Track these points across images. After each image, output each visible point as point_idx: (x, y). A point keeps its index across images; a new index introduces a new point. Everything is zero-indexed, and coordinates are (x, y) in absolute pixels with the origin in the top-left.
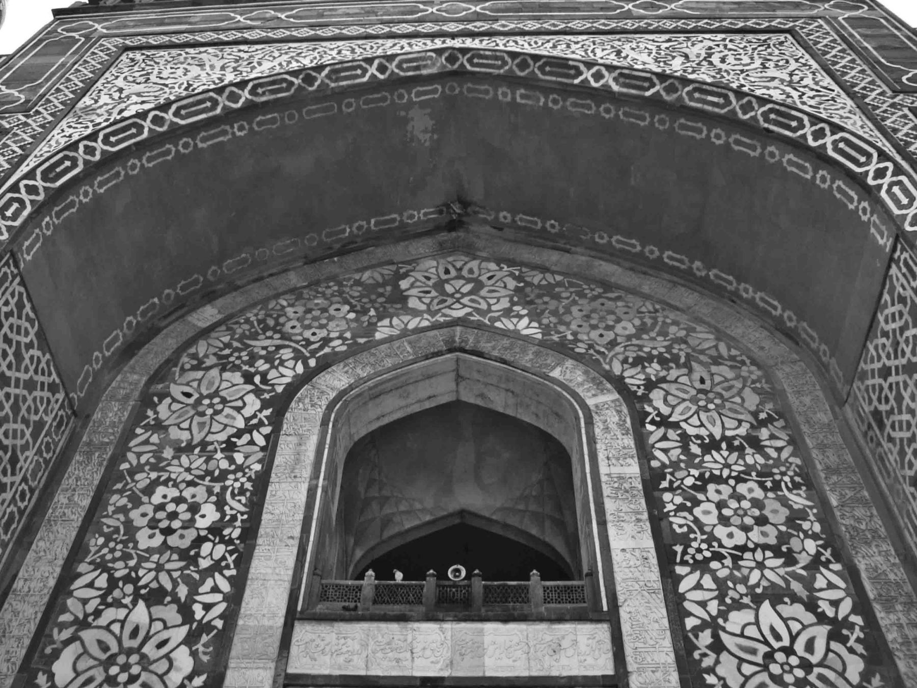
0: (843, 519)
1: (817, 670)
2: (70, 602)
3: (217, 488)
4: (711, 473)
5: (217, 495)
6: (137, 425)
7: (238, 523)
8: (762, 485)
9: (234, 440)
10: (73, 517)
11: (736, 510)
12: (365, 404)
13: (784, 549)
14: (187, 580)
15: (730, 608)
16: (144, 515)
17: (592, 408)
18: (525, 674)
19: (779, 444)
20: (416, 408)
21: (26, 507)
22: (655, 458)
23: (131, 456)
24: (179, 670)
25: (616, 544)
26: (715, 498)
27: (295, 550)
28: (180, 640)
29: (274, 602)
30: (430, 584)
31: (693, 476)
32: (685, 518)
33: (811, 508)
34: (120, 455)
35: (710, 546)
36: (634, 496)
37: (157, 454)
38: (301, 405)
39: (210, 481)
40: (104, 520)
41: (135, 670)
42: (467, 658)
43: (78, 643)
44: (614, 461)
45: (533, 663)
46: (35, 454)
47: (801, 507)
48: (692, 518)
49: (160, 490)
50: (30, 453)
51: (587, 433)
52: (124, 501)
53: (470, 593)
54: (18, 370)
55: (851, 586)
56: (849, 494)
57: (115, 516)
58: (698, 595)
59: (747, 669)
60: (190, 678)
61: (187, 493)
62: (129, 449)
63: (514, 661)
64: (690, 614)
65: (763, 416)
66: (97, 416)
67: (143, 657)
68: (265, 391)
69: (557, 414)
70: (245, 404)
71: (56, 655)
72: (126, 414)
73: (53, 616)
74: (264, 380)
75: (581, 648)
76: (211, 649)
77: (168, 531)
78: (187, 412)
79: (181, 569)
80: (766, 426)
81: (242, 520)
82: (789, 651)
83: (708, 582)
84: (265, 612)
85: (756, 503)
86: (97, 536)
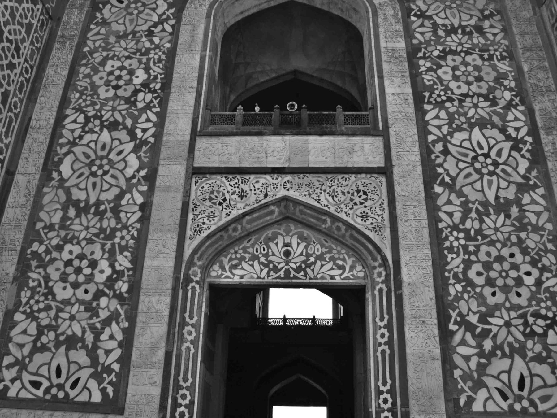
1: (501, 167)
2: (64, 131)
3: (144, 59)
4: (450, 48)
5: (145, 64)
6: (91, 22)
7: (159, 80)
8: (481, 57)
9: (152, 29)
11: (463, 72)
12: (233, 3)
13: (491, 96)
14: (131, 115)
16: (101, 78)
17: (377, 5)
18: (332, 165)
21: (30, 78)
22: (416, 38)
23: (89, 43)
24: (131, 167)
25: (389, 90)
26: (452, 64)
27: (194, 95)
28: (130, 150)
29: (183, 125)
30: (276, 113)
32: (432, 76)
34: (82, 42)
35: (446, 93)
36: (401, 61)
37: (106, 40)
38: (193, 6)
39: (140, 55)
40: (77, 83)
41: (106, 168)
43: (72, 154)
44: (389, 39)
45: (337, 159)
48: (436, 76)
49: (110, 63)
50: (27, 44)
51: (373, 21)
53: (300, 119)
55: (529, 119)
56: (536, 63)
58: (436, 122)
59: (462, 165)
60: (138, 171)
61: (127, 63)
62: (88, 39)
64: (431, 133)
65: (487, 12)
66: (65, 18)
67: (110, 160)
69: (355, 9)
70: (157, 6)
71: (61, 161)
72: (83, 16)
73: (56, 140)
75: (365, 150)
77: (117, 87)
78: (122, 13)
79: (126, 109)
80: (488, 19)
81: (161, 79)
82: (487, 156)
83: (443, 114)
84: (179, 131)
85: (477, 68)
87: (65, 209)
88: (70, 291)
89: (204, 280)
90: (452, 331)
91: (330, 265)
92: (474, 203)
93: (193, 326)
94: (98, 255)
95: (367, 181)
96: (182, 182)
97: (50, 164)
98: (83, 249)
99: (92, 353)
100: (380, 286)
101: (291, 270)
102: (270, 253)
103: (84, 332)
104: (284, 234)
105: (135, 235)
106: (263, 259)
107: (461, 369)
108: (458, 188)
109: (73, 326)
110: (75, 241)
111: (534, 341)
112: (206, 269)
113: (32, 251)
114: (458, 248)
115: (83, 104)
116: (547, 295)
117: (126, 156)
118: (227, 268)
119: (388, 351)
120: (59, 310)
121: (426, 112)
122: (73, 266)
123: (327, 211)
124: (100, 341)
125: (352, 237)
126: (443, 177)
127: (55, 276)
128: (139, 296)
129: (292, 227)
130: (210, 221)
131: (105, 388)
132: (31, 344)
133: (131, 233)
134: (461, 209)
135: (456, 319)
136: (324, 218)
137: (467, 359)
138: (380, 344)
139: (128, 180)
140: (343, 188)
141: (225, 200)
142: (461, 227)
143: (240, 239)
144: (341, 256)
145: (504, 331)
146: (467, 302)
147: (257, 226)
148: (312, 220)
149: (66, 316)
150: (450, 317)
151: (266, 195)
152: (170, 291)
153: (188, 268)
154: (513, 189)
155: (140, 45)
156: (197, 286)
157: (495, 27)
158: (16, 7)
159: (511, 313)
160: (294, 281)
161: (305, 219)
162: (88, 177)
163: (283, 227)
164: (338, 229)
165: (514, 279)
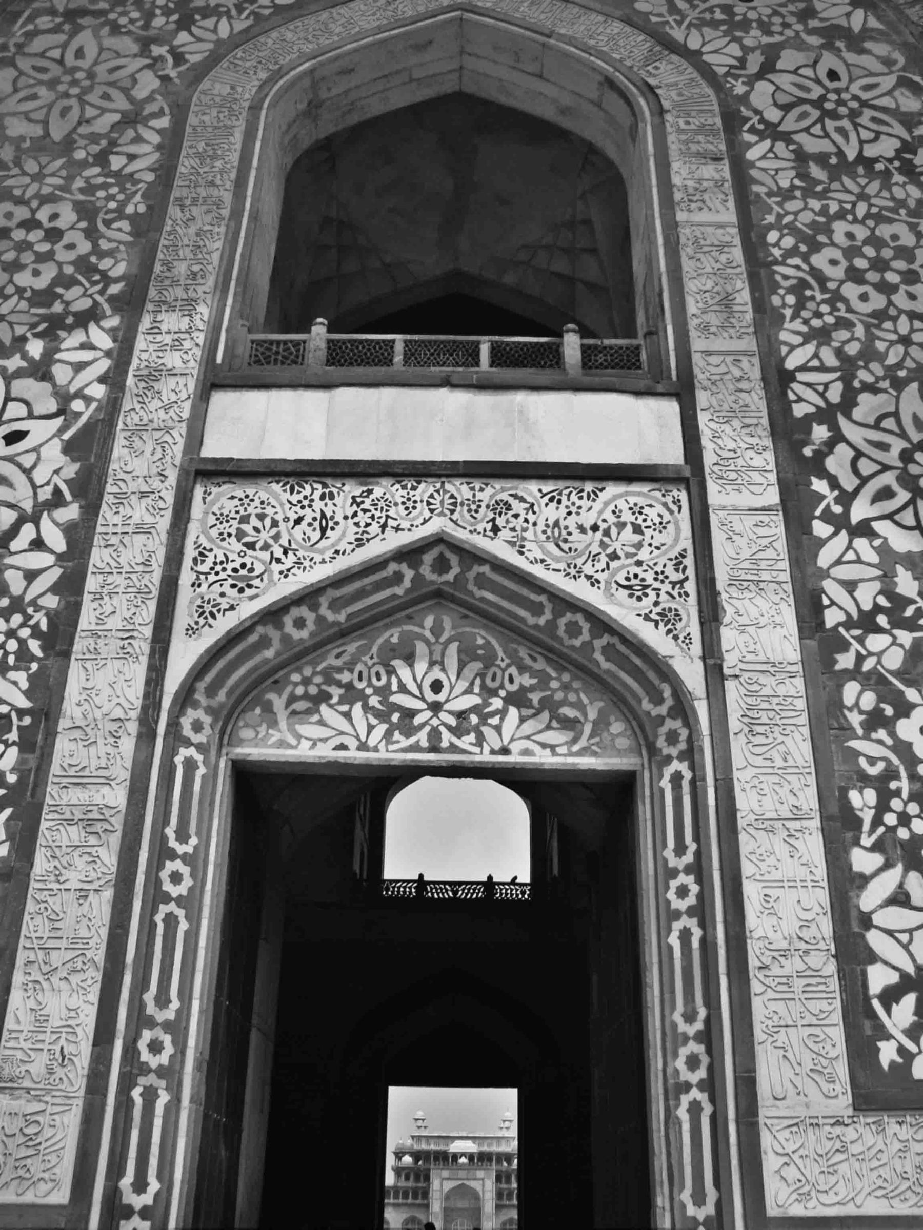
102: (395, 687)
105: (44, 626)
133: (32, 622)
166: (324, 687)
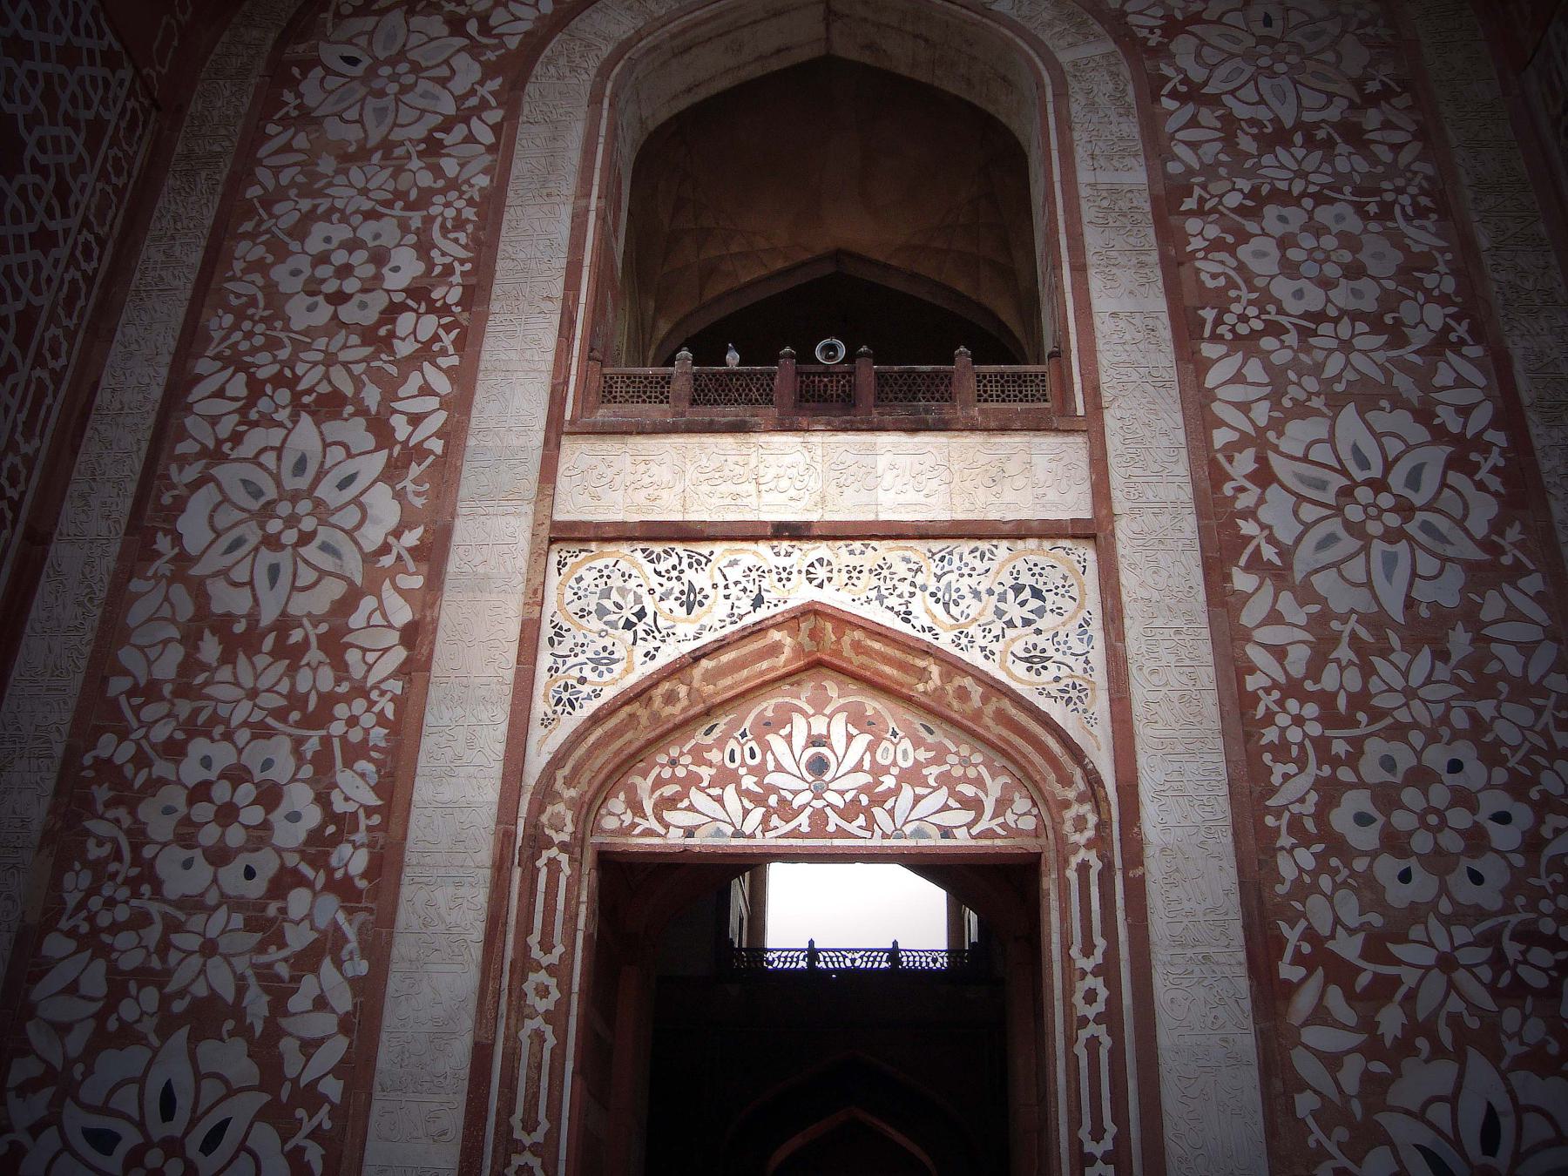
0: (1496, 271)
1: (1420, 516)
2: (189, 422)
3: (416, 220)
5: (417, 232)
7: (456, 279)
8: (1360, 209)
9: (438, 135)
10: (176, 283)
11: (1311, 251)
13: (1388, 319)
14: (378, 377)
15: (1290, 415)
17: (1066, 68)
18: (945, 516)
19: (1397, 137)
20: (756, 71)
21: (96, 271)
22: (1175, 158)
23: (262, 174)
25: (1102, 303)
26: (1277, 229)
27: (556, 319)
30: (784, 371)
31: (1241, 191)
32: (1222, 262)
33: (1442, 251)
34: (242, 176)
35: (1263, 311)
36: (1135, 223)
38: (552, 70)
39: (405, 209)
41: (308, 524)
42: (848, 492)
43: (212, 485)
46: (98, 180)
47: (1426, 249)
48: (1235, 264)
49: (319, 230)
50: (89, 178)
52: (260, 251)
53: (853, 386)
54: (43, 29)
57: (248, 277)
58: (1236, 393)
60: (397, 533)
62: (260, 162)
63: (927, 496)
64: (1221, 423)
65: (1373, 87)
67: (318, 503)
68: (486, 46)
69: (1004, 79)
70: (453, 72)
71: (180, 505)
72: (247, 101)
74: (485, 29)
76: (427, 486)
77: (339, 298)
80: (1376, 105)
82: (1379, 485)
83: (1254, 371)
85: (1349, 241)
86: (220, 312)
87: (191, 639)
88: (202, 872)
89: (583, 839)
90: (1287, 982)
91: (941, 796)
92: (1344, 619)
93: (551, 970)
94: (283, 769)
95: (1043, 561)
96: (522, 563)
97: (151, 512)
98: (240, 751)
99: (265, 1049)
100: (1082, 854)
101: (828, 810)
102: (771, 765)
103: (241, 990)
104: (811, 711)
105: (390, 713)
106: (749, 782)
107: (1315, 1091)
108: (1298, 576)
109: (210, 972)
110: (218, 730)
111: (1522, 1009)
112: (588, 810)
113: (96, 758)
114: (1301, 746)
115: (244, 346)
116: (1559, 878)
117: (362, 494)
118: (648, 806)
119: (1106, 1042)
120: (173, 926)
121: (1203, 366)
122: (210, 801)
123: (929, 644)
124: (286, 1014)
125: (1002, 718)
126: (1258, 546)
127: (161, 827)
128: (398, 885)
129: (833, 691)
130: (601, 675)
131: (299, 1150)
132: (91, 1024)
133: (376, 709)
134: (1310, 638)
135: (1297, 949)
136: (921, 663)
137: (1332, 1061)
138: (1083, 1022)
139: (371, 558)
140: (975, 579)
141: (641, 614)
142: (1309, 686)
143: (685, 725)
144: (972, 773)
145: (1437, 980)
146: (1329, 899)
147: (731, 687)
148: (887, 670)
149: (191, 942)
150: (1281, 942)
151: (758, 602)
152: (488, 873)
153: (538, 806)
154: (1455, 577)
155: (404, 181)
156: (564, 858)
157: (1397, 128)
158: (61, 76)
159: (1453, 928)
160: (837, 842)
161: (866, 668)
162: (256, 549)
163: (807, 690)
164: (963, 694)
165: (1461, 833)
166: (693, 768)
